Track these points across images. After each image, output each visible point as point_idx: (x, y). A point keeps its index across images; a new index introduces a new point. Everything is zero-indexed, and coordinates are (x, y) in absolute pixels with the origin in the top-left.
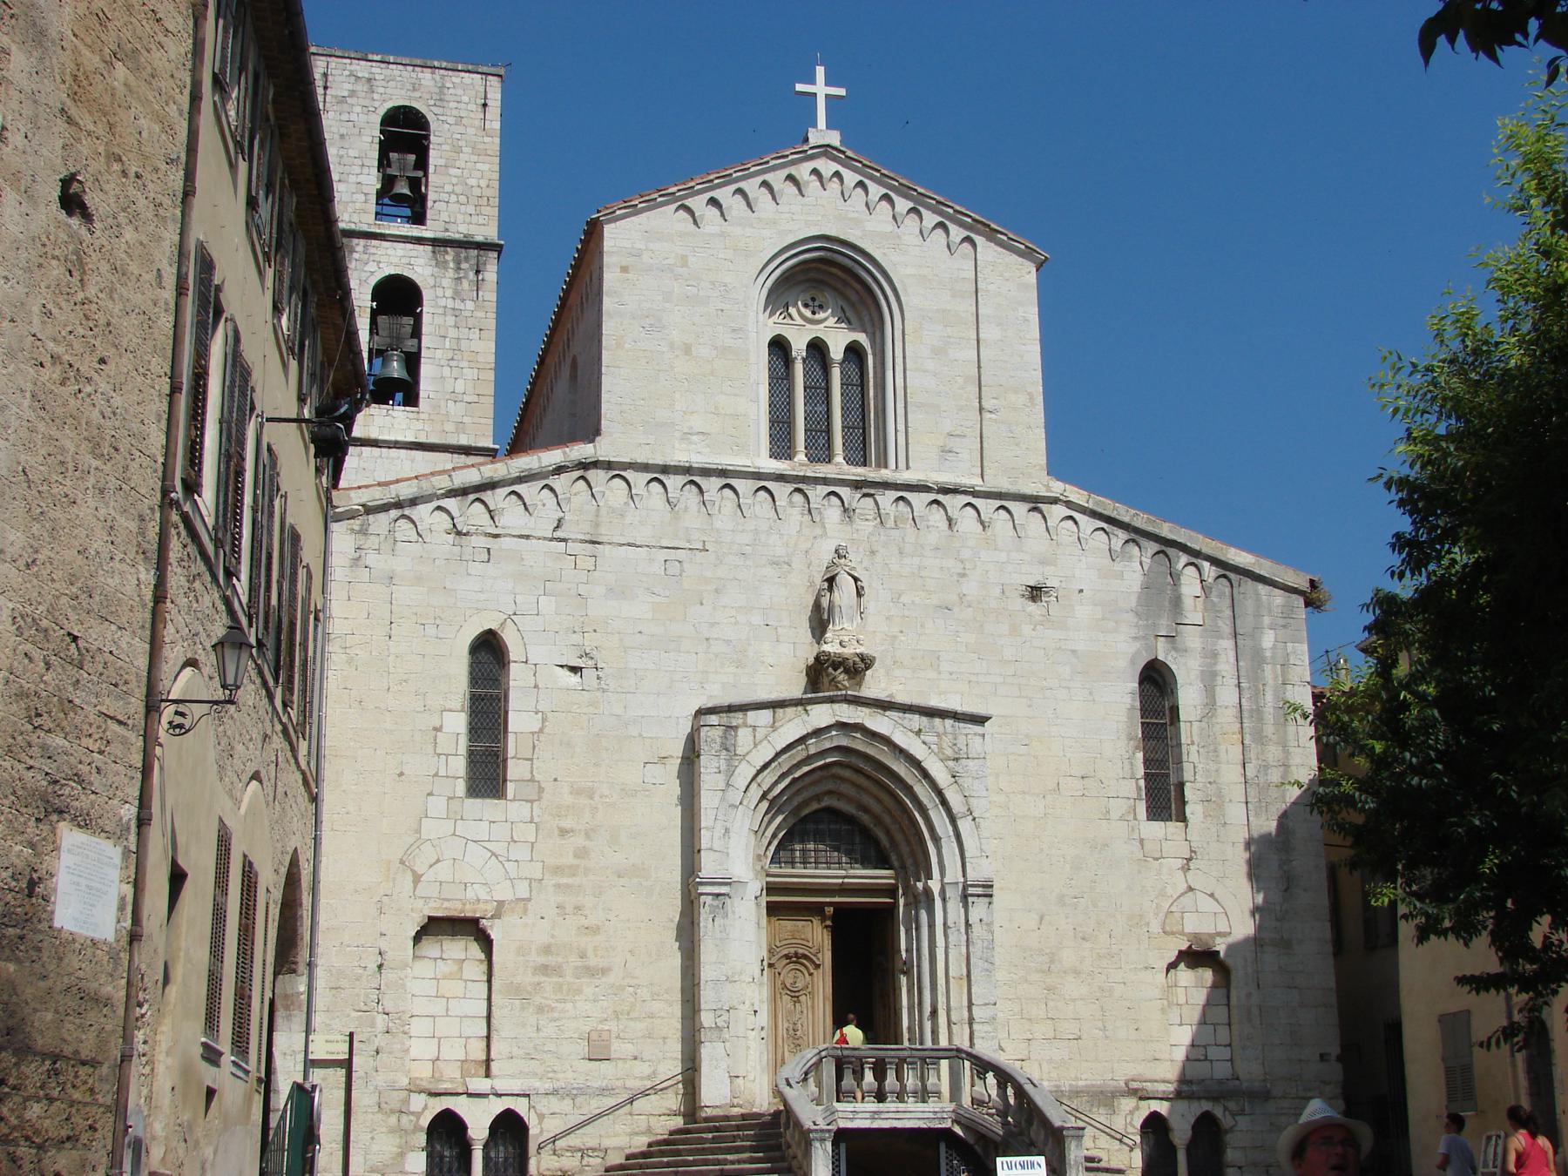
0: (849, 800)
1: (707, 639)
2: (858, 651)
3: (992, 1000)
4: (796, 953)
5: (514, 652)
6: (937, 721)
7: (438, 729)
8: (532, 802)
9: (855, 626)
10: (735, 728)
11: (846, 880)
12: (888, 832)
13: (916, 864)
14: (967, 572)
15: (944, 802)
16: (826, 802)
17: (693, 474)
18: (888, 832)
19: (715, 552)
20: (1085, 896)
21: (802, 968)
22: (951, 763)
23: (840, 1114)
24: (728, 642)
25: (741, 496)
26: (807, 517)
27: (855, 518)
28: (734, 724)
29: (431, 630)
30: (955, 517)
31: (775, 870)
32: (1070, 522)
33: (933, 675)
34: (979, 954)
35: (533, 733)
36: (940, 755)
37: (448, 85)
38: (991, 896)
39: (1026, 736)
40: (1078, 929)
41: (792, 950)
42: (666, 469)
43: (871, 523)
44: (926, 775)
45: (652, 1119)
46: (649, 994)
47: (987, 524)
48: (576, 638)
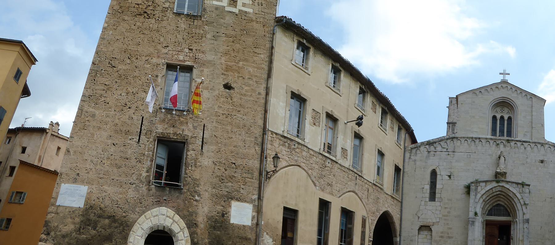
1: (475, 170)
5: (438, 173)
6: (519, 185)
7: (423, 188)
8: (440, 202)
16: (499, 202)
17: (473, 139)
24: (479, 170)
29: (423, 170)
35: (441, 188)
42: (468, 138)
48: (450, 170)
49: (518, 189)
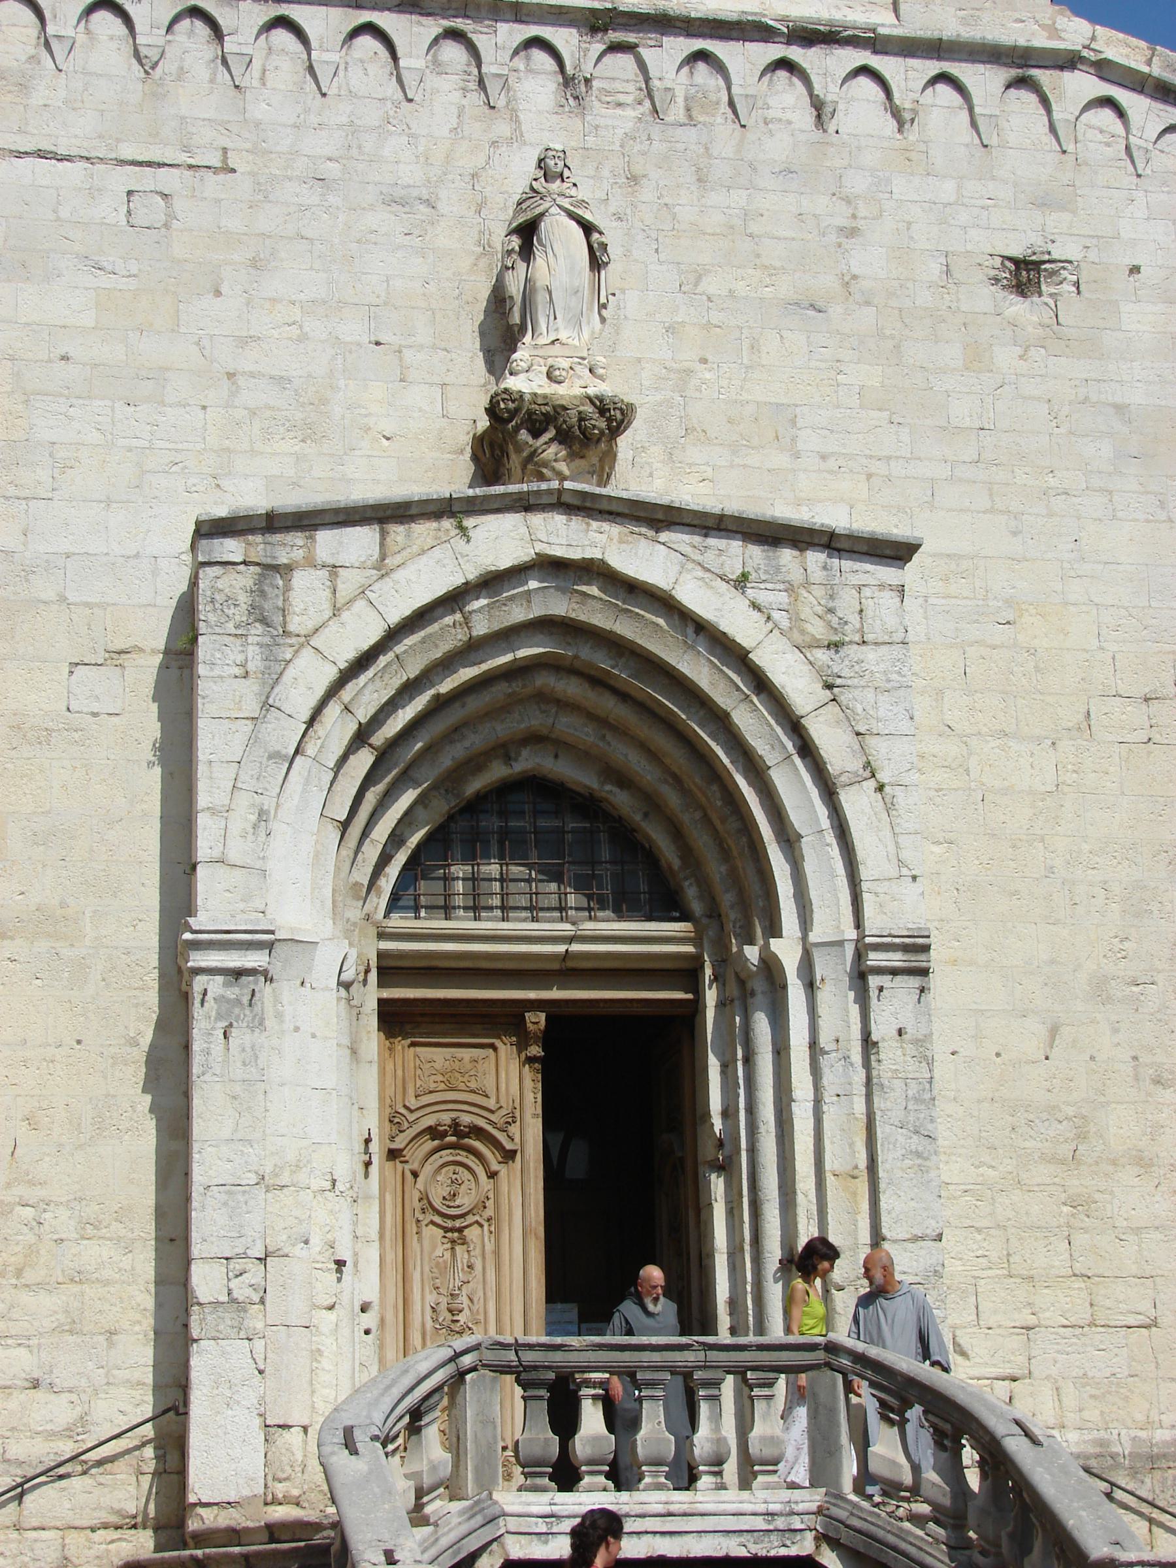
0: (584, 756)
1: (231, 376)
2: (591, 391)
3: (932, 1227)
4: (455, 1124)
6: (787, 555)
9: (586, 334)
10: (285, 570)
11: (576, 947)
12: (677, 834)
13: (744, 904)
14: (860, 224)
15: (807, 749)
16: (527, 762)
18: (677, 834)
19: (252, 174)
20: (1159, 978)
21: (471, 1161)
22: (822, 656)
23: (513, 1524)
24: (281, 381)
25: (314, 44)
26: (477, 98)
27: (592, 101)
28: (283, 560)
30: (829, 98)
31: (400, 922)
32: (1107, 114)
33: (781, 460)
34: (897, 1114)
36: (796, 636)
38: (924, 972)
39: (1009, 602)
40: (1145, 1058)
41: (446, 1118)
43: (630, 113)
44: (761, 683)
45: (72, 1537)
46: (72, 1223)
47: (907, 116)
49: (783, 598)
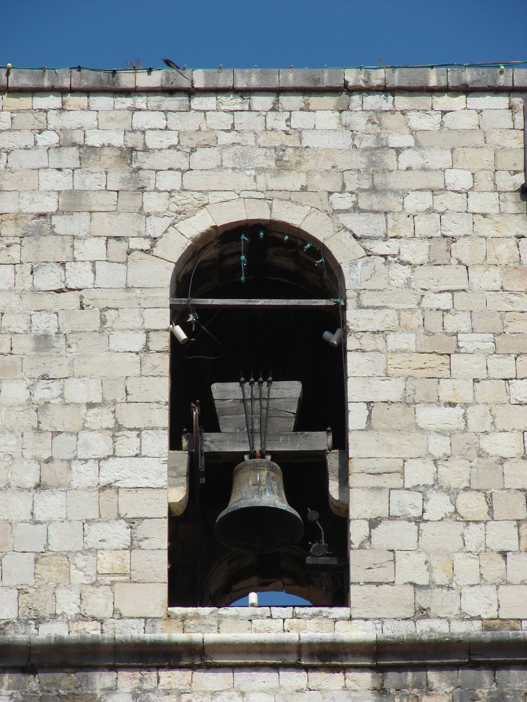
37: (395, 141)
